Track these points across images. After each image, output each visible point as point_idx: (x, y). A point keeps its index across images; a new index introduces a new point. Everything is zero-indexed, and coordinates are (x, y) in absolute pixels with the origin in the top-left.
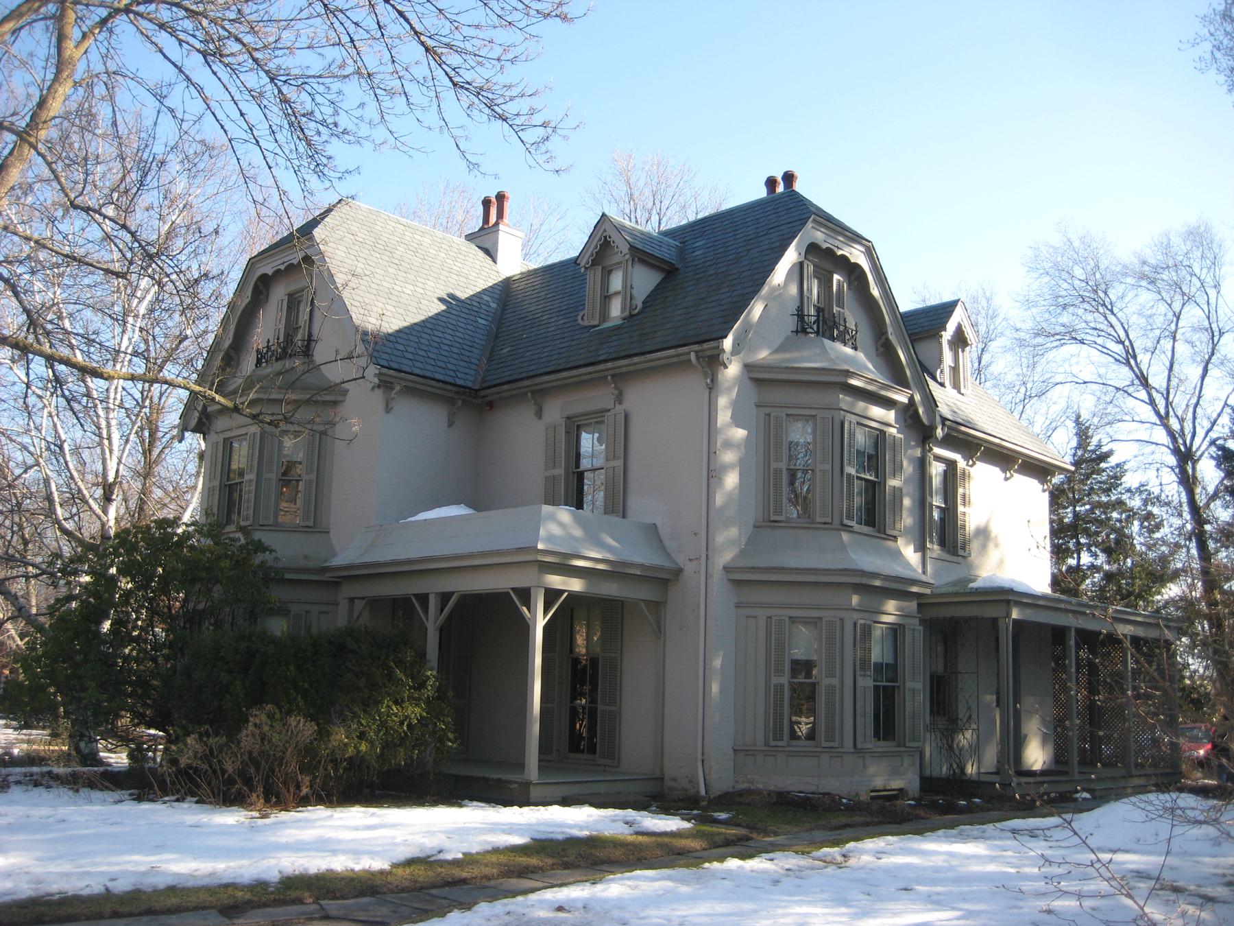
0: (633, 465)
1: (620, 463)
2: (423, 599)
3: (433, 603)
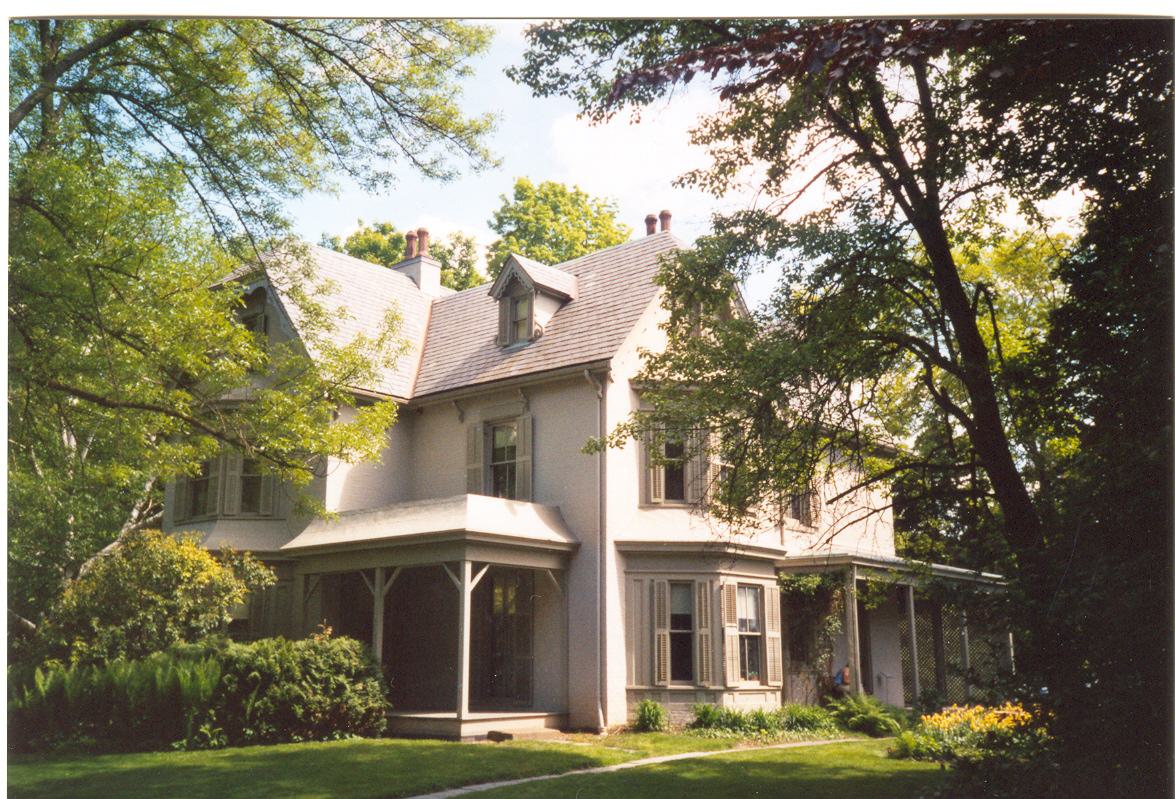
0: (539, 454)
1: (529, 458)
2: (371, 573)
3: (378, 575)
